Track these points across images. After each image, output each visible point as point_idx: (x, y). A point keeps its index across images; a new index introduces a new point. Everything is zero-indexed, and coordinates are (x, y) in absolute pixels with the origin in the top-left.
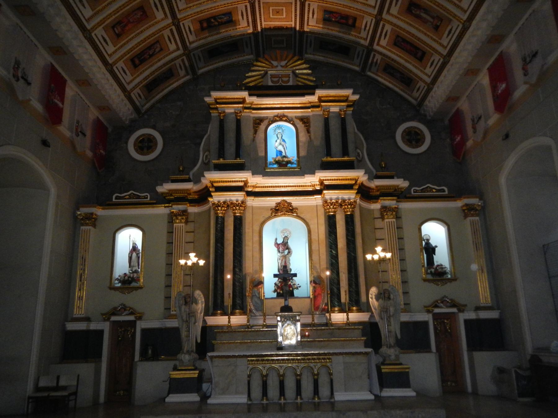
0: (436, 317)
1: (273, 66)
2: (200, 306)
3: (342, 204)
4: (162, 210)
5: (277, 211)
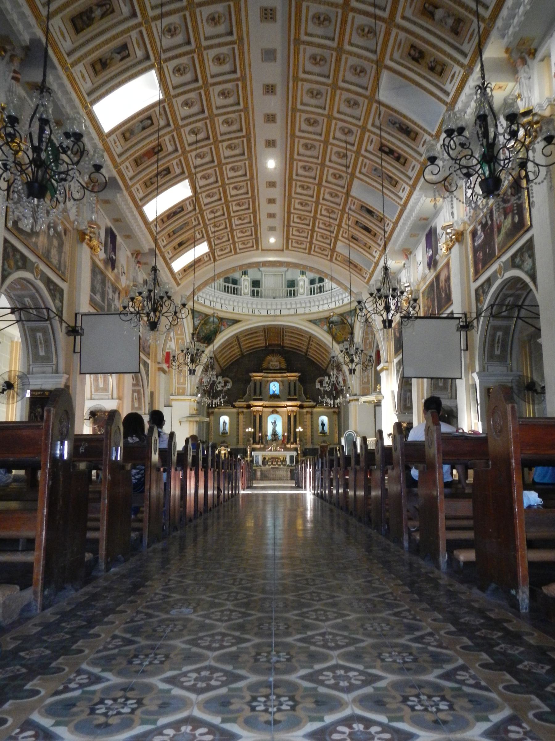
0: (321, 447)
1: (271, 361)
2: (252, 442)
3: (292, 411)
4: (234, 410)
5: (272, 413)
